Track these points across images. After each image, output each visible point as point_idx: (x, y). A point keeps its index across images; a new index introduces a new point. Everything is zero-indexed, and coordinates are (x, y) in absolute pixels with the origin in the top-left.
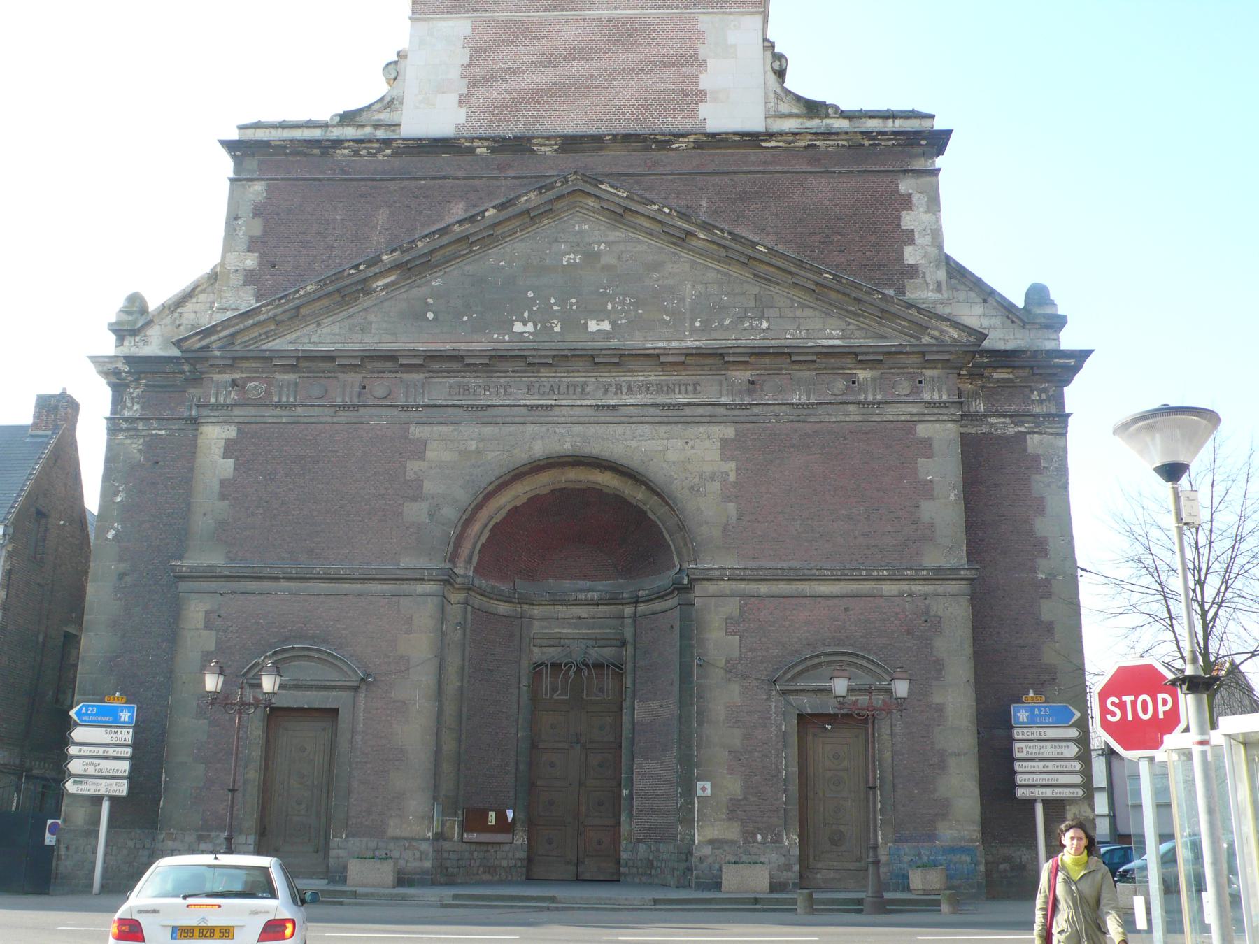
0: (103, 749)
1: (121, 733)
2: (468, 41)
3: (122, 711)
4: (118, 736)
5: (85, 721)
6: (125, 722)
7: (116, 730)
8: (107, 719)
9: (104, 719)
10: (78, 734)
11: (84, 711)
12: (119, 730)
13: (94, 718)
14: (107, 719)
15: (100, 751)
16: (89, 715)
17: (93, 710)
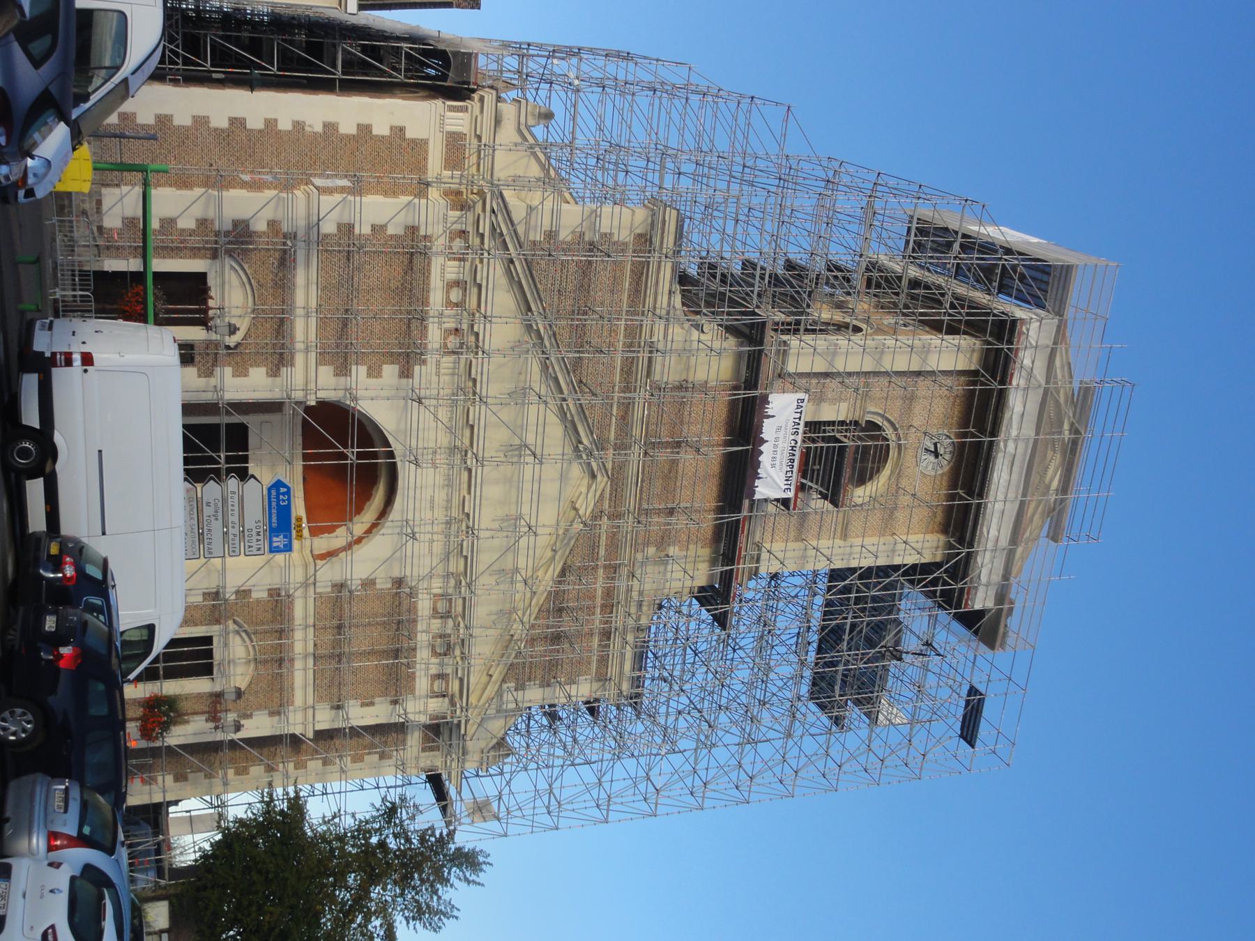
1: (258, 540)
3: (285, 537)
4: (255, 537)
7: (262, 533)
11: (283, 490)
13: (274, 504)
17: (284, 501)
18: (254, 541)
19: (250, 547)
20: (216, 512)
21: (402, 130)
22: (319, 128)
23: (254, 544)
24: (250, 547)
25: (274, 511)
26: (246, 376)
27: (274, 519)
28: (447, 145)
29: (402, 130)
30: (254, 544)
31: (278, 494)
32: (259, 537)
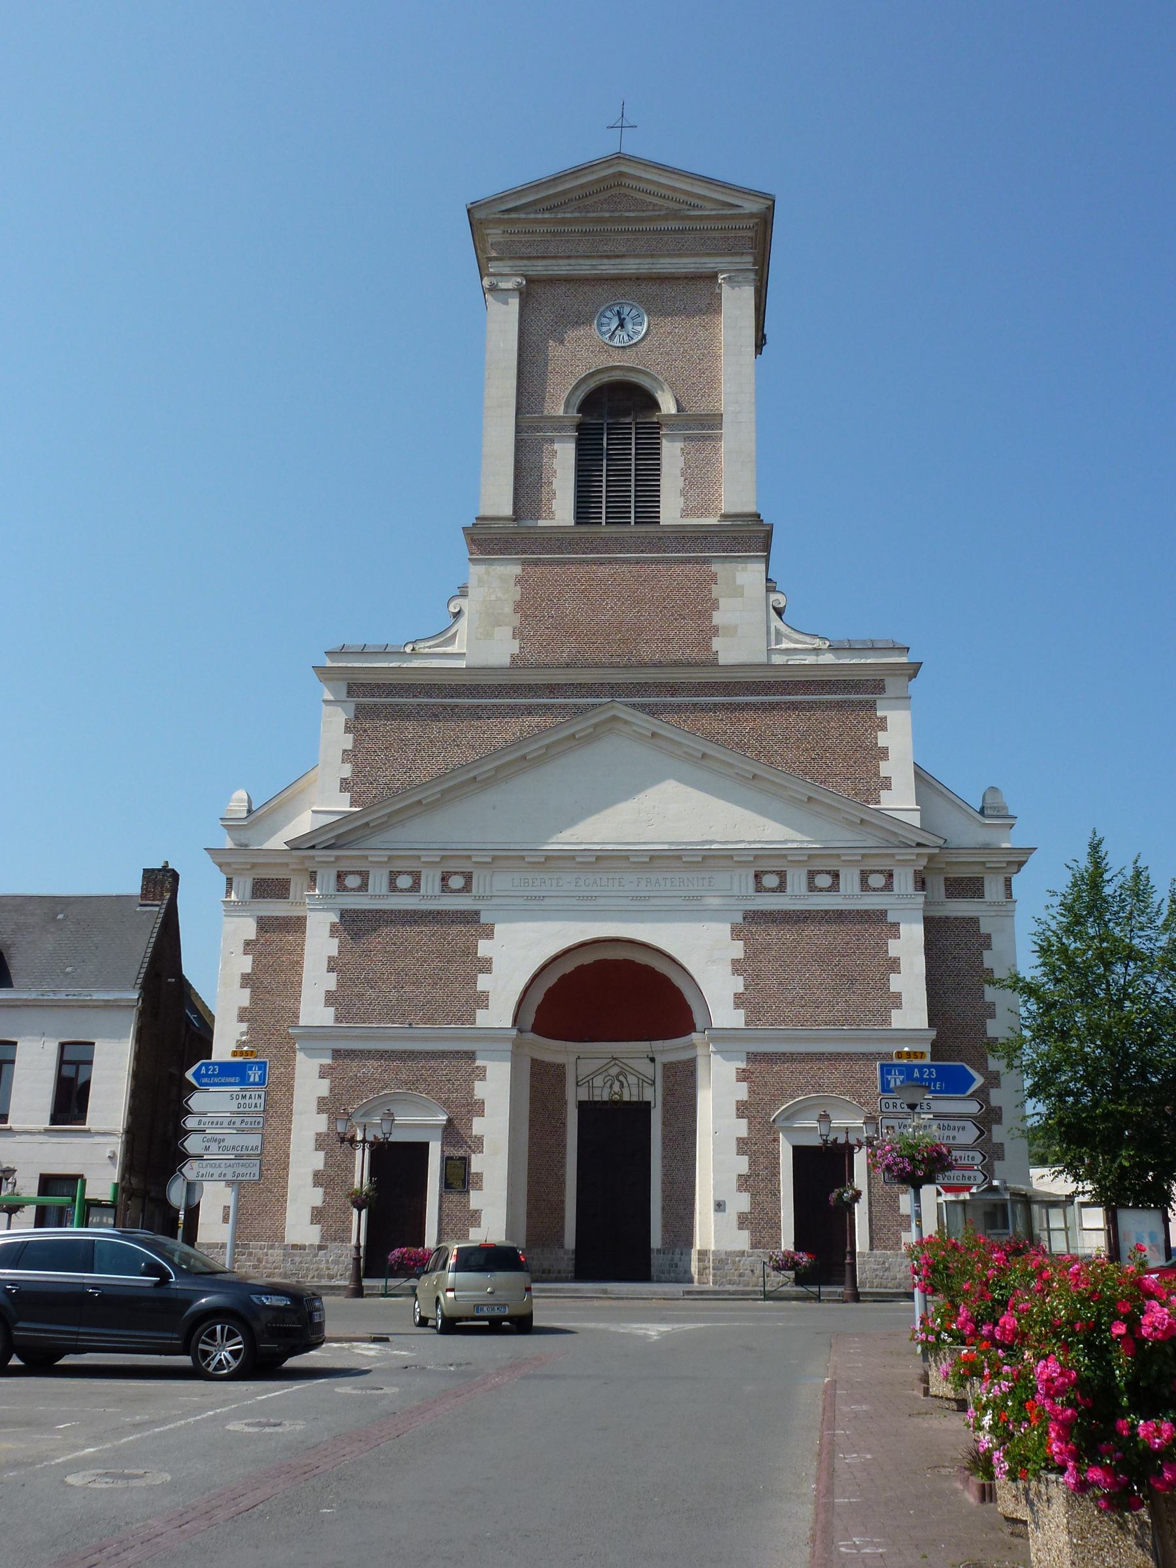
1: (250, 1097)
2: (519, 581)
3: (251, 1069)
4: (247, 1101)
7: (244, 1093)
10: (196, 1101)
11: (203, 1071)
16: (210, 1076)
17: (214, 1070)
18: (250, 1101)
19: (256, 1106)
20: (216, 1141)
21: (248, 943)
22: (244, 1027)
23: (253, 1101)
24: (256, 1106)
25: (223, 1080)
26: (483, 1103)
27: (232, 1080)
28: (264, 897)
29: (248, 943)
30: (253, 1101)
31: (207, 1075)
32: (248, 1097)
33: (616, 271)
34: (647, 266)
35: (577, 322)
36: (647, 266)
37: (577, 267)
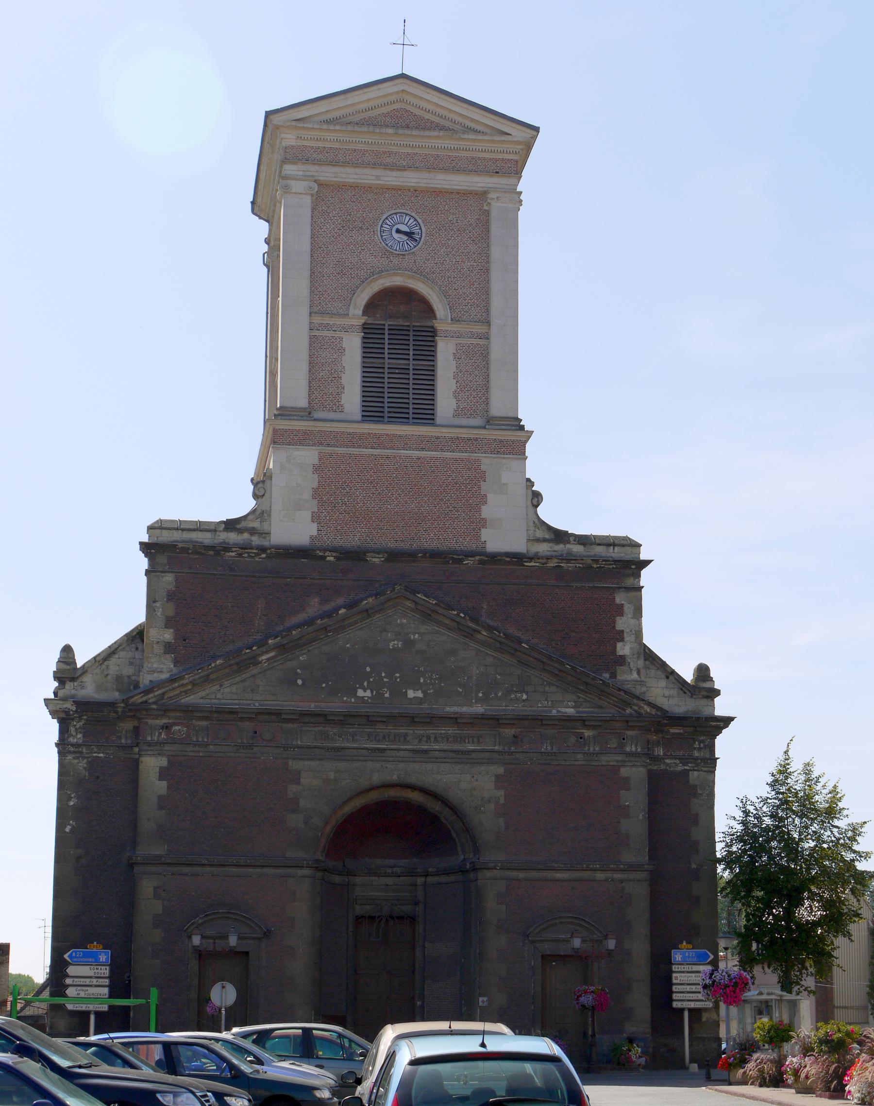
0: (89, 980)
4: (99, 971)
5: (76, 962)
6: (103, 962)
7: (97, 967)
8: (90, 960)
9: (88, 960)
10: (71, 970)
11: (74, 954)
12: (100, 967)
13: (81, 960)
14: (90, 960)
15: (88, 981)
17: (80, 954)
20: (83, 990)
23: (103, 971)
25: (85, 960)
30: (103, 971)
31: (76, 957)
33: (397, 183)
34: (425, 181)
35: (361, 228)
36: (425, 181)
37: (363, 177)
